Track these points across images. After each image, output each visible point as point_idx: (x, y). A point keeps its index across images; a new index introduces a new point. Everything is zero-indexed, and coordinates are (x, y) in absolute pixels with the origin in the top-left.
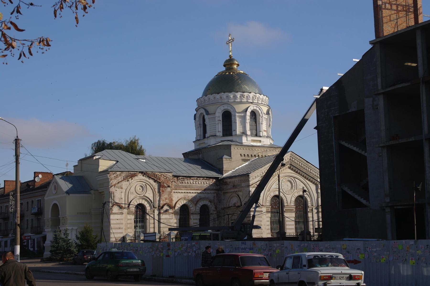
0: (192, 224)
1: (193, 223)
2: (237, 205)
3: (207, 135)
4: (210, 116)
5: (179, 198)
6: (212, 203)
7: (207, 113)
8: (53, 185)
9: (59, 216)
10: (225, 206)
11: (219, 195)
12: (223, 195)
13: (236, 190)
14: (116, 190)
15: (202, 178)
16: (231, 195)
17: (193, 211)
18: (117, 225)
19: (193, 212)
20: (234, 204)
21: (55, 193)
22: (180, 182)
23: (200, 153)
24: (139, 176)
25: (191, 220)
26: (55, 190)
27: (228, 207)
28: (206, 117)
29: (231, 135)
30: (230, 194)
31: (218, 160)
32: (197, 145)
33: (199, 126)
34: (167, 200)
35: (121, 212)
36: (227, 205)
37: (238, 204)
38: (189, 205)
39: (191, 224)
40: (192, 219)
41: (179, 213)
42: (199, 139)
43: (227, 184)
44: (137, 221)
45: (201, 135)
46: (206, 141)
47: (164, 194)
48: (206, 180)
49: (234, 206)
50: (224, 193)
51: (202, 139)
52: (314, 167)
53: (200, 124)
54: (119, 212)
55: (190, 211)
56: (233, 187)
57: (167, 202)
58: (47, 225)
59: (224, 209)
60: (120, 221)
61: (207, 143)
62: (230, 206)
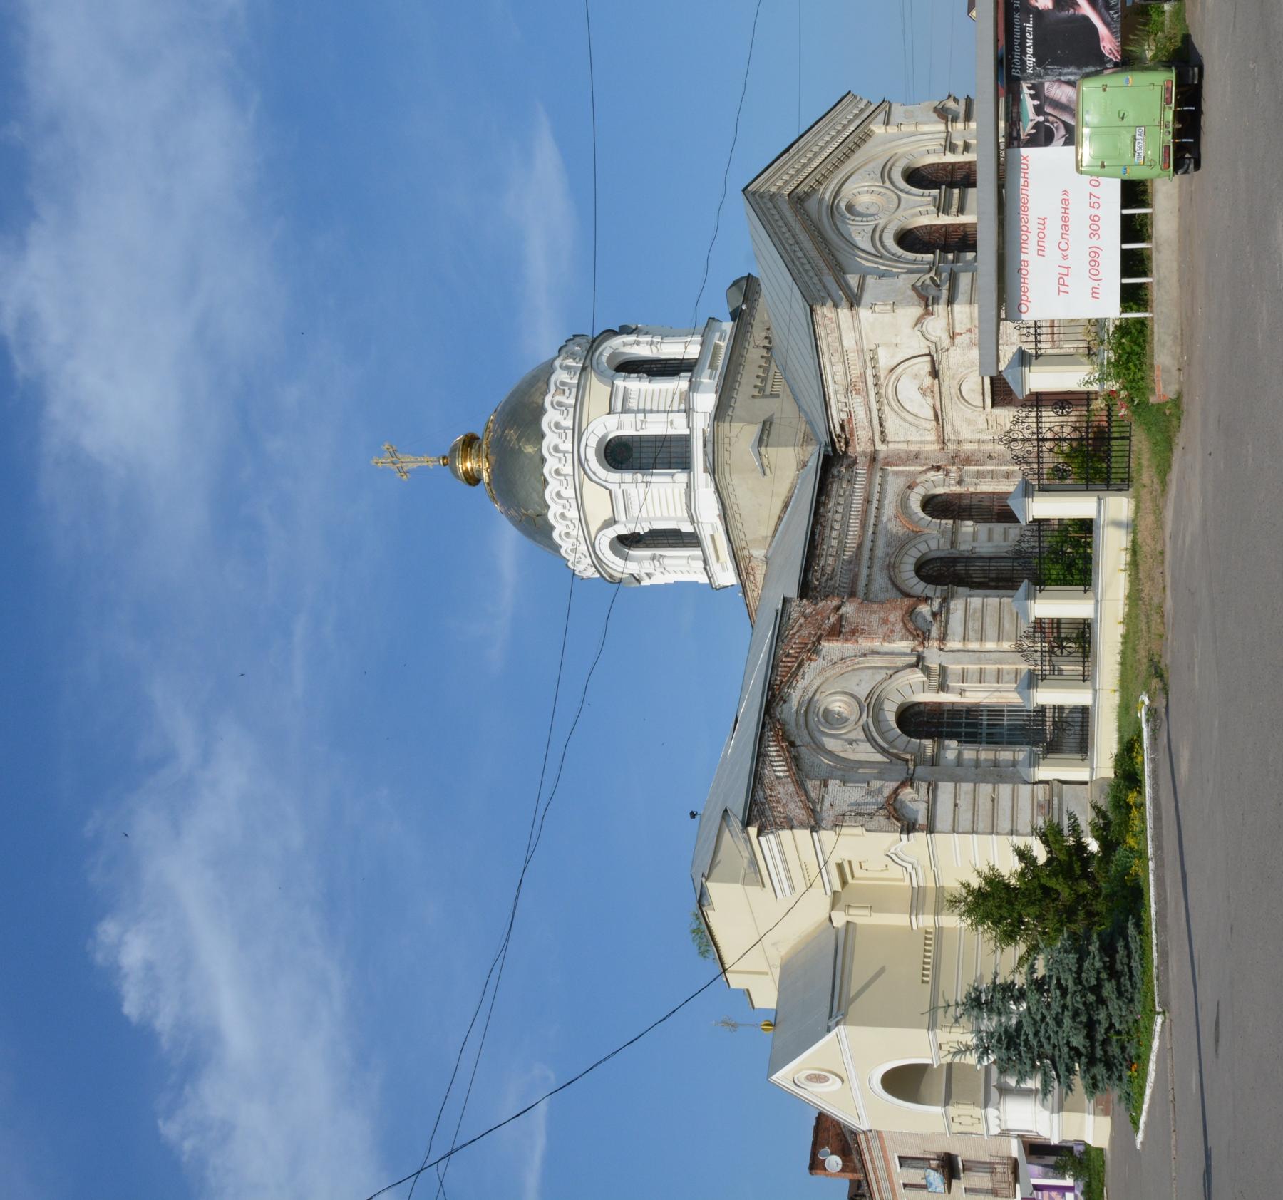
0: (993, 547)
1: (990, 544)
2: (928, 380)
3: (686, 528)
4: (621, 516)
5: (890, 586)
6: (918, 481)
7: (612, 522)
8: (809, 1089)
9: (935, 1066)
10: (932, 436)
11: (890, 460)
12: (891, 445)
13: (871, 381)
14: (832, 805)
15: (822, 510)
16: (889, 405)
17: (942, 541)
18: (981, 807)
19: (949, 542)
20: (924, 395)
21: (839, 1081)
22: (826, 581)
23: (746, 553)
24: (783, 716)
25: (977, 550)
26: (825, 1079)
27: (934, 423)
28: (621, 530)
29: (685, 441)
30: (886, 409)
31: (767, 471)
32: (724, 571)
33: (656, 562)
34: (892, 618)
35: (926, 790)
36: (929, 427)
37: (922, 373)
38: (919, 555)
39: (991, 550)
40: (975, 544)
41: (946, 587)
42: (701, 564)
43: (850, 421)
44: (967, 735)
45: (689, 557)
46: (705, 534)
47: (865, 627)
48: (828, 496)
49: (932, 392)
50: (883, 441)
51: (701, 553)
52: (809, 133)
53: (653, 558)
54: (926, 798)
55: (943, 550)
56: (858, 393)
57: (899, 619)
58: (973, 1124)
59: (944, 443)
60: (962, 797)
61: (712, 524)
62: (931, 415)
